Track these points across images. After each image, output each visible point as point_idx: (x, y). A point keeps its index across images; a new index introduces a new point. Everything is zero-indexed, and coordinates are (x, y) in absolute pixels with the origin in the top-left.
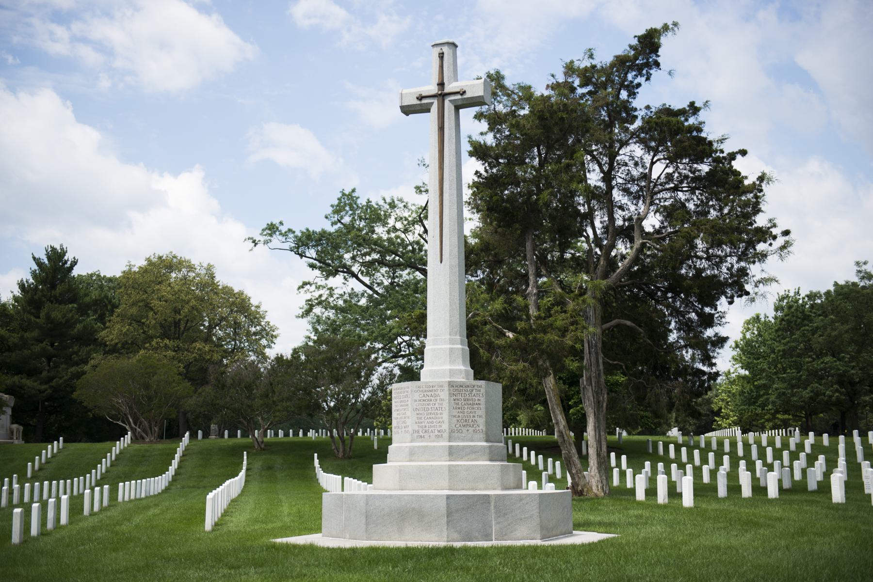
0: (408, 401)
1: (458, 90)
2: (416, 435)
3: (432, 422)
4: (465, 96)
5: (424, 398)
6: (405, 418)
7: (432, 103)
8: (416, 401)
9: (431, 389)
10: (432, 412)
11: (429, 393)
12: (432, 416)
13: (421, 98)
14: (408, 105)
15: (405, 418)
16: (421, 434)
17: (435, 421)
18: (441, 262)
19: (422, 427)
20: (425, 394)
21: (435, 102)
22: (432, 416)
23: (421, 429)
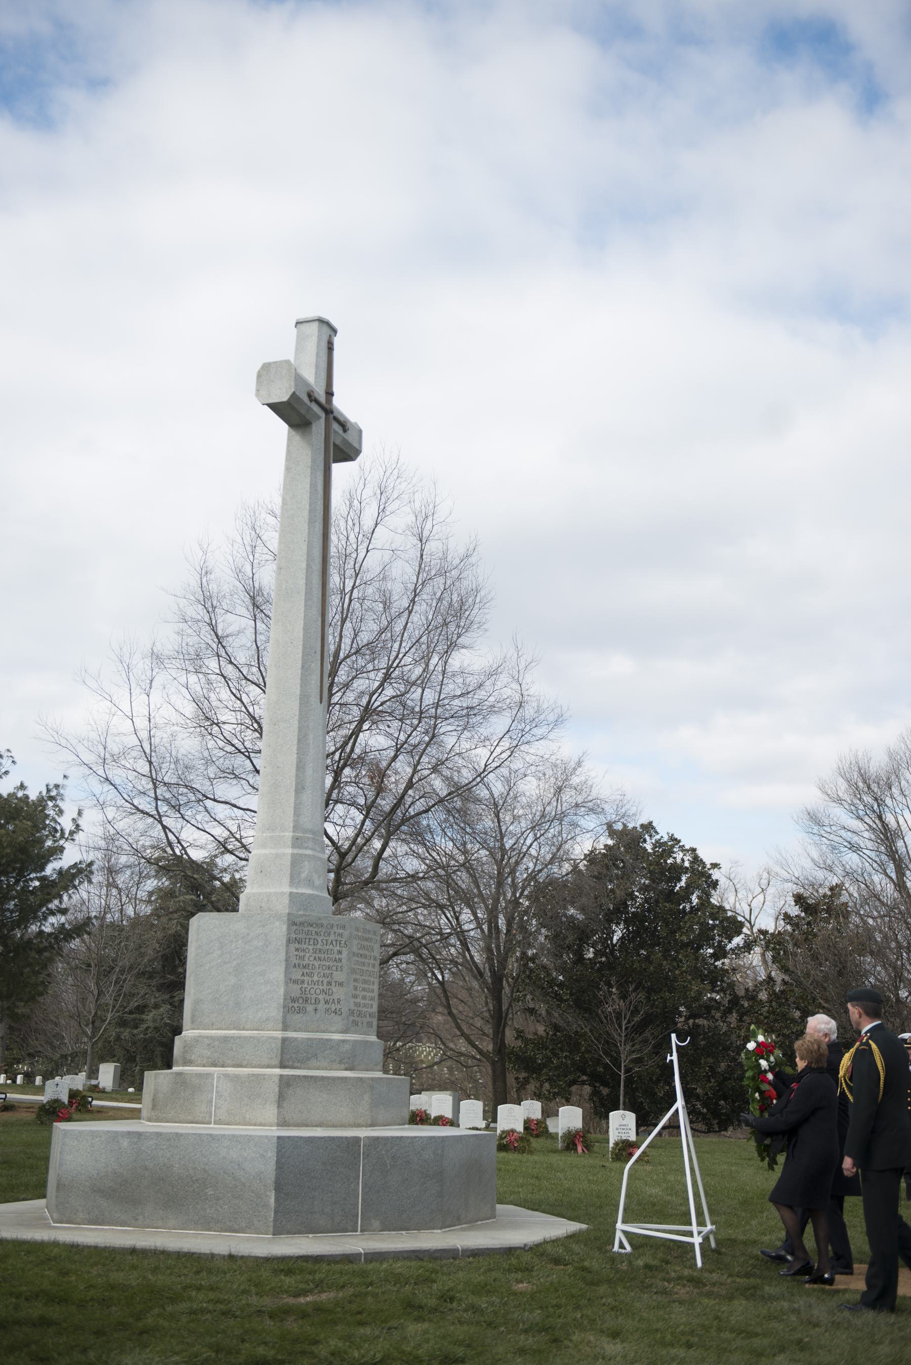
0: (340, 952)
1: (342, 419)
2: (351, 1018)
3: (364, 998)
4: (345, 436)
5: (361, 952)
6: (329, 983)
7: (319, 417)
8: (354, 954)
9: (367, 936)
10: (367, 978)
11: (366, 943)
12: (366, 986)
13: (310, 396)
14: (299, 398)
15: (329, 983)
16: (356, 1018)
17: (368, 994)
18: (321, 703)
19: (357, 1005)
20: (363, 943)
21: (323, 415)
22: (366, 986)
23: (356, 1008)
